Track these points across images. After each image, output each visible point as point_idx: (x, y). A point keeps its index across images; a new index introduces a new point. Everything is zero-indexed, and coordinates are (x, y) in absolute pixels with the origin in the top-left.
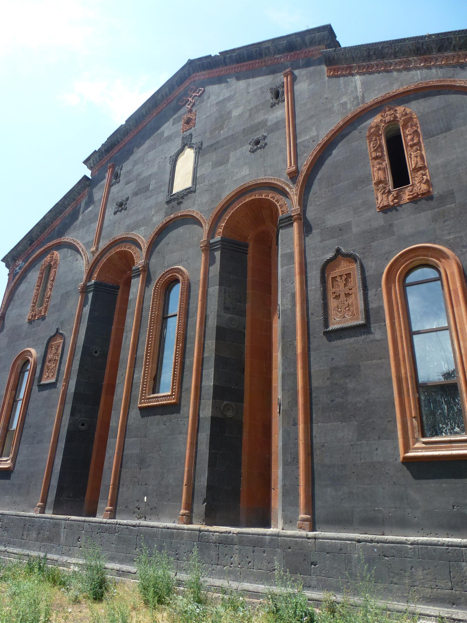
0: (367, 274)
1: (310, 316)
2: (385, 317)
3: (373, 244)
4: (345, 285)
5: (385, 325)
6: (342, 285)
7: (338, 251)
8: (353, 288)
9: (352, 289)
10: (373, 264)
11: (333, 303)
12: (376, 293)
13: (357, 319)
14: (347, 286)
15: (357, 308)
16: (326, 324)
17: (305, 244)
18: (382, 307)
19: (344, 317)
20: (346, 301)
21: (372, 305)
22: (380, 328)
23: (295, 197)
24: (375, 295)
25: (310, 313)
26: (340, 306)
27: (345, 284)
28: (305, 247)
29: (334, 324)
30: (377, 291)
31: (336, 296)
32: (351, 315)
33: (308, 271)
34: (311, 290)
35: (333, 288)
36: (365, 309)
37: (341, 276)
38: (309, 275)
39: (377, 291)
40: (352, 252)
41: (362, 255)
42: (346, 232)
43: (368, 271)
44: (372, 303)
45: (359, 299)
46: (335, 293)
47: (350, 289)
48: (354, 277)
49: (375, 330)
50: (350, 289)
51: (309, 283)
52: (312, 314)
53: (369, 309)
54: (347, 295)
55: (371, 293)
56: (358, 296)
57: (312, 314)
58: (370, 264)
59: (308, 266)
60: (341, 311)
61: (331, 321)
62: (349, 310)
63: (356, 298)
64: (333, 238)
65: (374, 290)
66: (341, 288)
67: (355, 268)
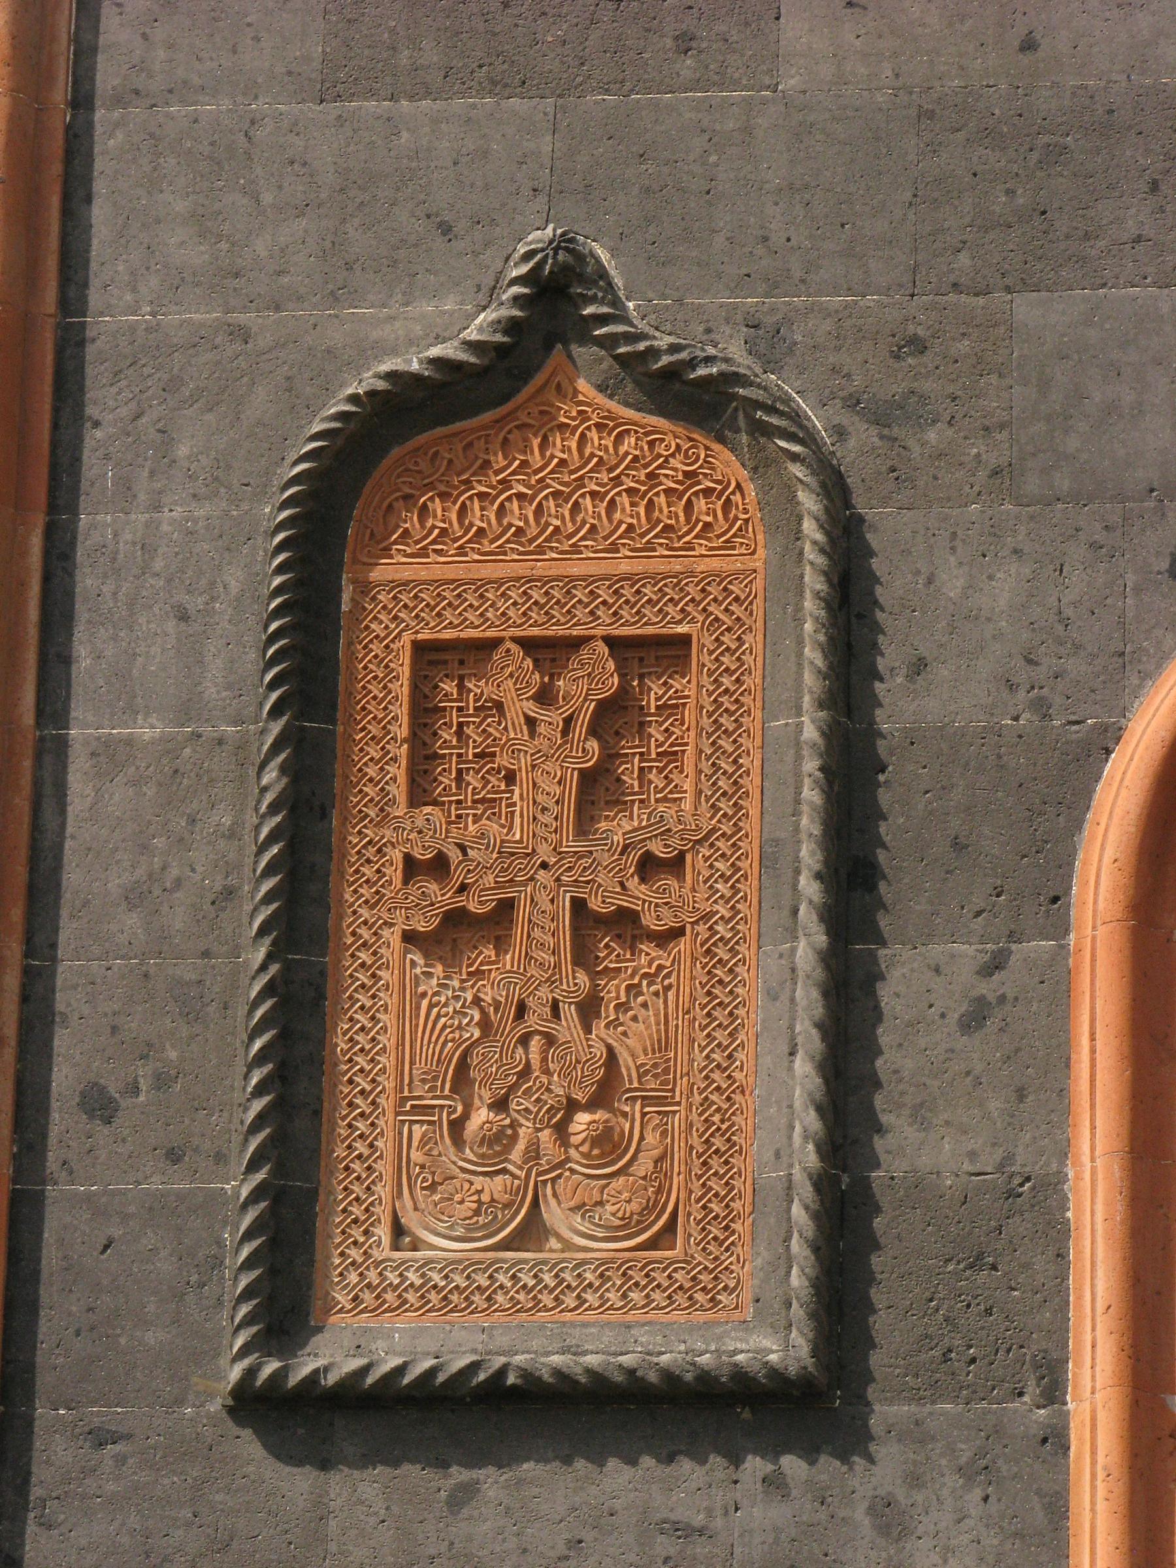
0: (897, 708)
1: (63, 1120)
2: (1059, 1330)
3: (1025, 308)
4: (597, 790)
5: (1055, 1440)
6: (548, 778)
7: (557, 298)
8: (696, 863)
9: (676, 865)
10: (1004, 587)
11: (398, 1011)
12: (987, 988)
13: (706, 1289)
14: (618, 802)
15: (719, 1146)
16: (285, 1303)
17: (85, 54)
18: (1033, 1200)
19: (533, 1231)
20: (589, 1009)
21: (919, 1150)
22: (978, 1471)
23: (715, 370)
24: (976, 1016)
25: (64, 1079)
26: (491, 1069)
27: (589, 779)
28: (82, 101)
29: (383, 1300)
30: (995, 965)
31: (455, 919)
32: (627, 1226)
33: (98, 469)
34: (114, 756)
35: (419, 794)
36: (823, 1183)
37: (550, 652)
38: (99, 525)
39: (995, 965)
40: (742, 361)
41: (862, 434)
42: (685, 43)
43: (919, 666)
44: (920, 1115)
45: (754, 1016)
46: (439, 866)
47: (648, 867)
48: (726, 711)
49: (914, 1480)
50: (648, 867)
51: (90, 651)
52: (99, 1105)
53: (863, 1187)
54: (598, 929)
55: (920, 978)
56: (752, 983)
57: (99, 1105)
58: (953, 583)
59: (106, 400)
60: (501, 1140)
61: (352, 1258)
62: (607, 1144)
63: (718, 1002)
64: (496, 86)
65: (969, 952)
66: (517, 811)
67: (748, 573)
